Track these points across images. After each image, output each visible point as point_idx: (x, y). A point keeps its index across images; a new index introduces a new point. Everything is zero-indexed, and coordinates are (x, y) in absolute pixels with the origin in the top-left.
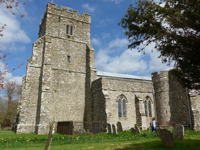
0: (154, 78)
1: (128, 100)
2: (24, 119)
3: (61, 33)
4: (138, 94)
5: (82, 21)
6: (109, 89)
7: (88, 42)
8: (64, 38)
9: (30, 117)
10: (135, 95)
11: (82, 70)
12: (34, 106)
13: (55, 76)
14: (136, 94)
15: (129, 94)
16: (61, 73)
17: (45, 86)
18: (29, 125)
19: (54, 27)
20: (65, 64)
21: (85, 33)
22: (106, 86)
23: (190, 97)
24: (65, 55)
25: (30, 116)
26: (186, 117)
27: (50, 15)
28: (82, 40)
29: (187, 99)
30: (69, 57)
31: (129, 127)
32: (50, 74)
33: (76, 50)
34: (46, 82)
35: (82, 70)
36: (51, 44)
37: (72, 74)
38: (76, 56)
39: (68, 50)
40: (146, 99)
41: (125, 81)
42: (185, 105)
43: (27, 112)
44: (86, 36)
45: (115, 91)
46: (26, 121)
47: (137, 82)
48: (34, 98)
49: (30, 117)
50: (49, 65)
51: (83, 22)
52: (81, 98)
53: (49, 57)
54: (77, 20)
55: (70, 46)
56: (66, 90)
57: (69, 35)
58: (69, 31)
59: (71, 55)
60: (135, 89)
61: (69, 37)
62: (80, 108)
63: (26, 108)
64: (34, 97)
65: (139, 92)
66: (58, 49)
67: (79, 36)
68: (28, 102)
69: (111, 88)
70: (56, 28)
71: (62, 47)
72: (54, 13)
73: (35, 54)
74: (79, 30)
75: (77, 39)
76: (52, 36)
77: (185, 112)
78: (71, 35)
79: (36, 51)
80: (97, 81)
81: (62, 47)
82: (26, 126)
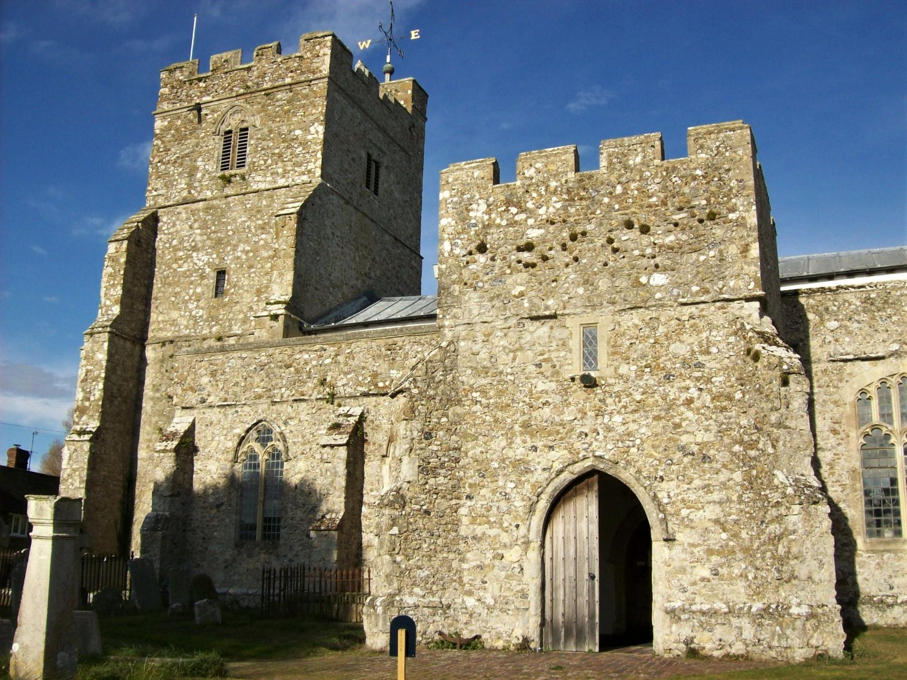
1: (293, 450)
3: (199, 175)
6: (203, 401)
8: (209, 194)
13: (163, 370)
15: (303, 417)
17: (85, 418)
20: (202, 308)
22: (192, 389)
24: (208, 270)
30: (221, 274)
34: (87, 404)
38: (247, 260)
45: (234, 410)
55: (229, 224)
58: (234, 156)
65: (366, 395)
66: (181, 254)
69: (210, 399)
71: (198, 238)
81: (198, 238)
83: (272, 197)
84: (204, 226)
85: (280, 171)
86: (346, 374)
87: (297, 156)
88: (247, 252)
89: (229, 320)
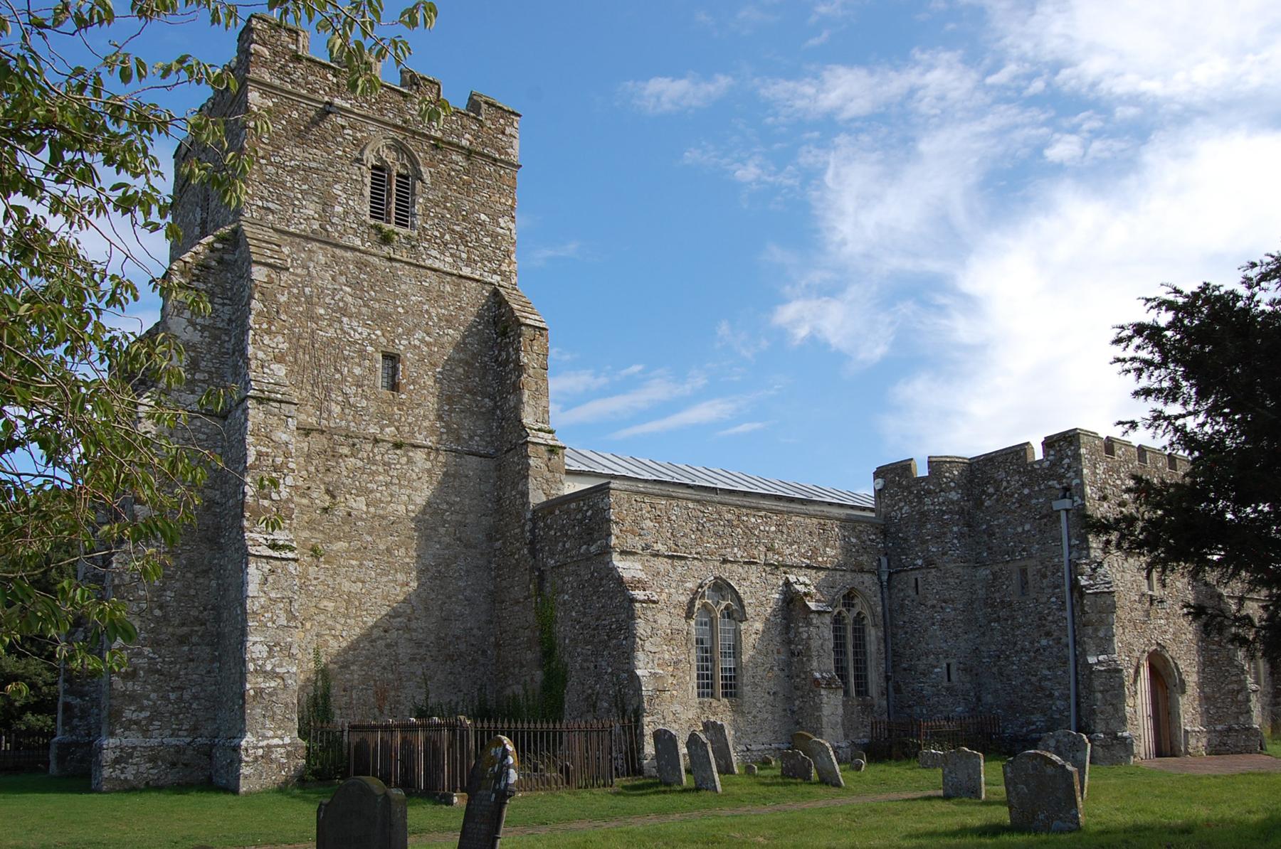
0: (892, 496)
2: (142, 709)
4: (801, 579)
5: (464, 143)
7: (502, 274)
9: (172, 696)
10: (787, 584)
11: (471, 438)
12: (195, 639)
14: (792, 578)
16: (345, 450)
18: (173, 741)
19: (293, 171)
21: (483, 217)
23: (1082, 595)
25: (173, 690)
26: (1051, 696)
27: (264, 94)
28: (469, 262)
29: (1062, 608)
30: (392, 359)
31: (753, 747)
32: (287, 455)
33: (430, 318)
35: (471, 438)
36: (285, 276)
37: (410, 461)
39: (384, 317)
40: (844, 605)
41: (737, 506)
42: (1048, 634)
43: (152, 671)
44: (494, 236)
46: (150, 720)
47: (798, 514)
48: (192, 592)
49: (172, 696)
50: (281, 402)
51: (469, 154)
52: (468, 593)
53: (279, 359)
54: (439, 134)
56: (382, 547)
57: (387, 227)
59: (401, 346)
60: (788, 552)
61: (386, 239)
62: (463, 647)
63: (147, 650)
64: (189, 587)
67: (447, 237)
68: (157, 612)
70: (305, 180)
72: (293, 82)
73: (186, 337)
74: (446, 198)
75: (434, 253)
76: (282, 226)
77: (1047, 672)
78: (403, 231)
79: (187, 314)
80: (573, 505)
82: (152, 749)
83: (459, 285)
84: (356, 285)
85: (464, 256)
86: (791, 545)
87: (485, 247)
88: (428, 344)
89: (410, 424)
